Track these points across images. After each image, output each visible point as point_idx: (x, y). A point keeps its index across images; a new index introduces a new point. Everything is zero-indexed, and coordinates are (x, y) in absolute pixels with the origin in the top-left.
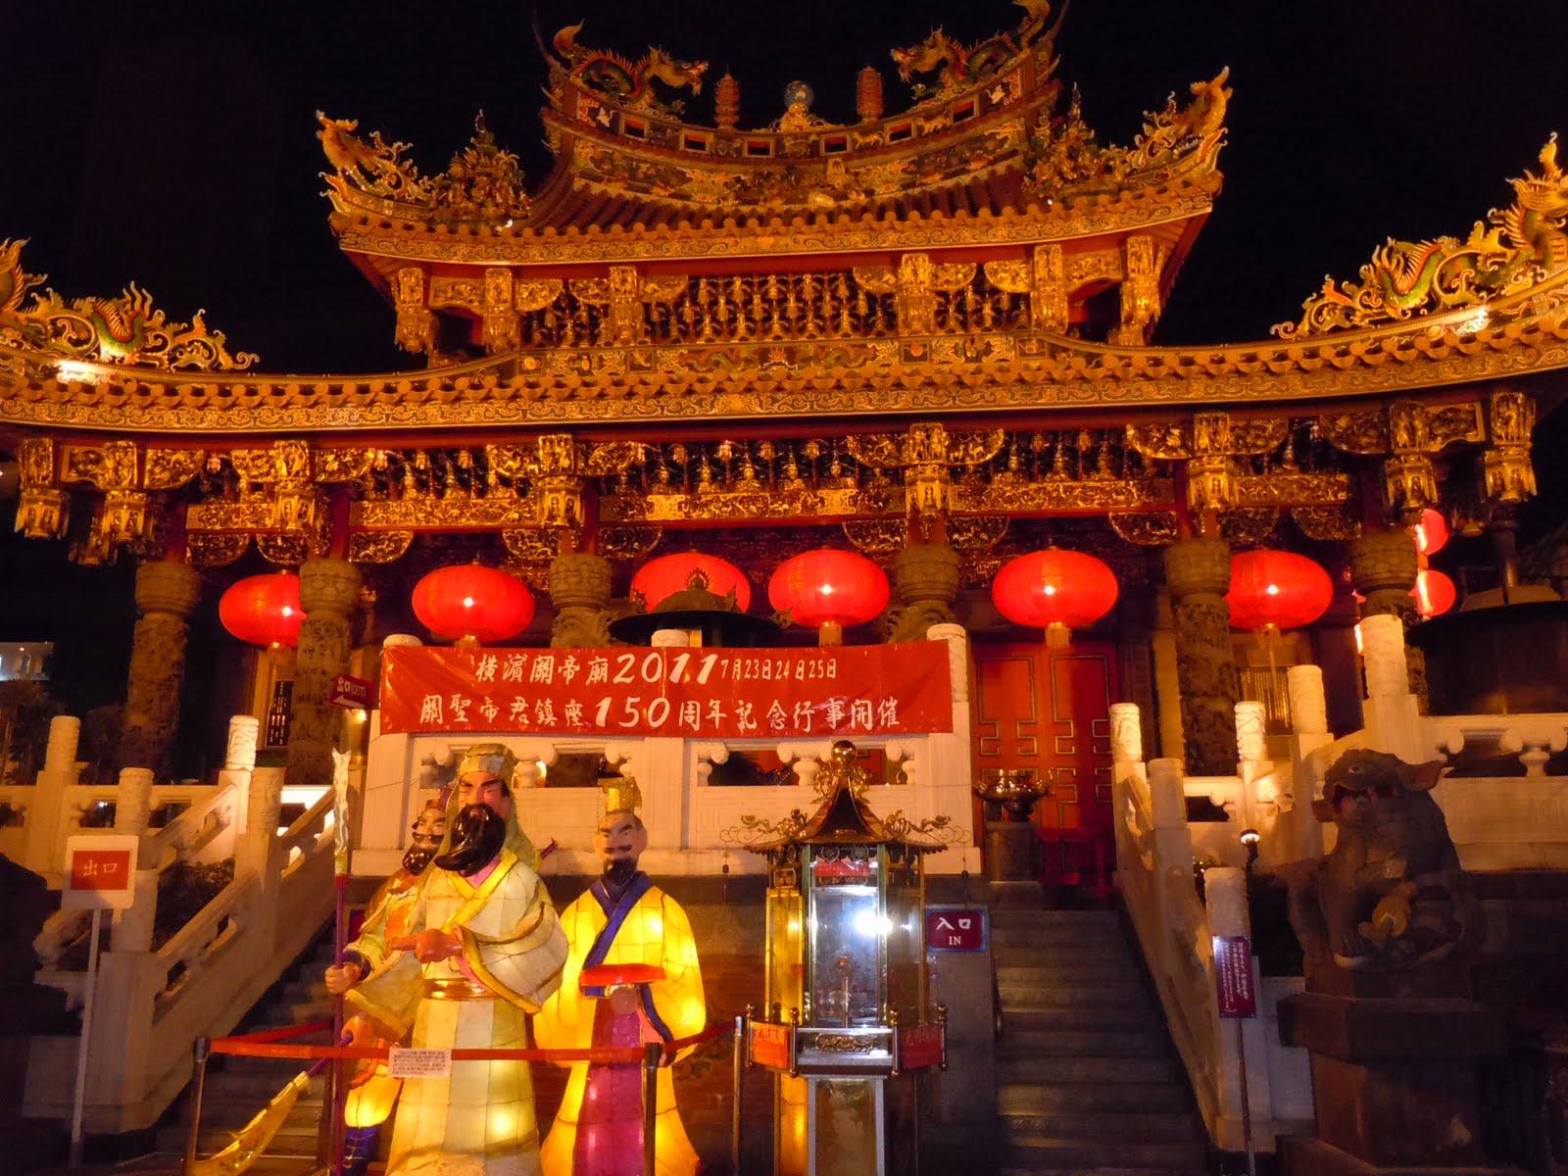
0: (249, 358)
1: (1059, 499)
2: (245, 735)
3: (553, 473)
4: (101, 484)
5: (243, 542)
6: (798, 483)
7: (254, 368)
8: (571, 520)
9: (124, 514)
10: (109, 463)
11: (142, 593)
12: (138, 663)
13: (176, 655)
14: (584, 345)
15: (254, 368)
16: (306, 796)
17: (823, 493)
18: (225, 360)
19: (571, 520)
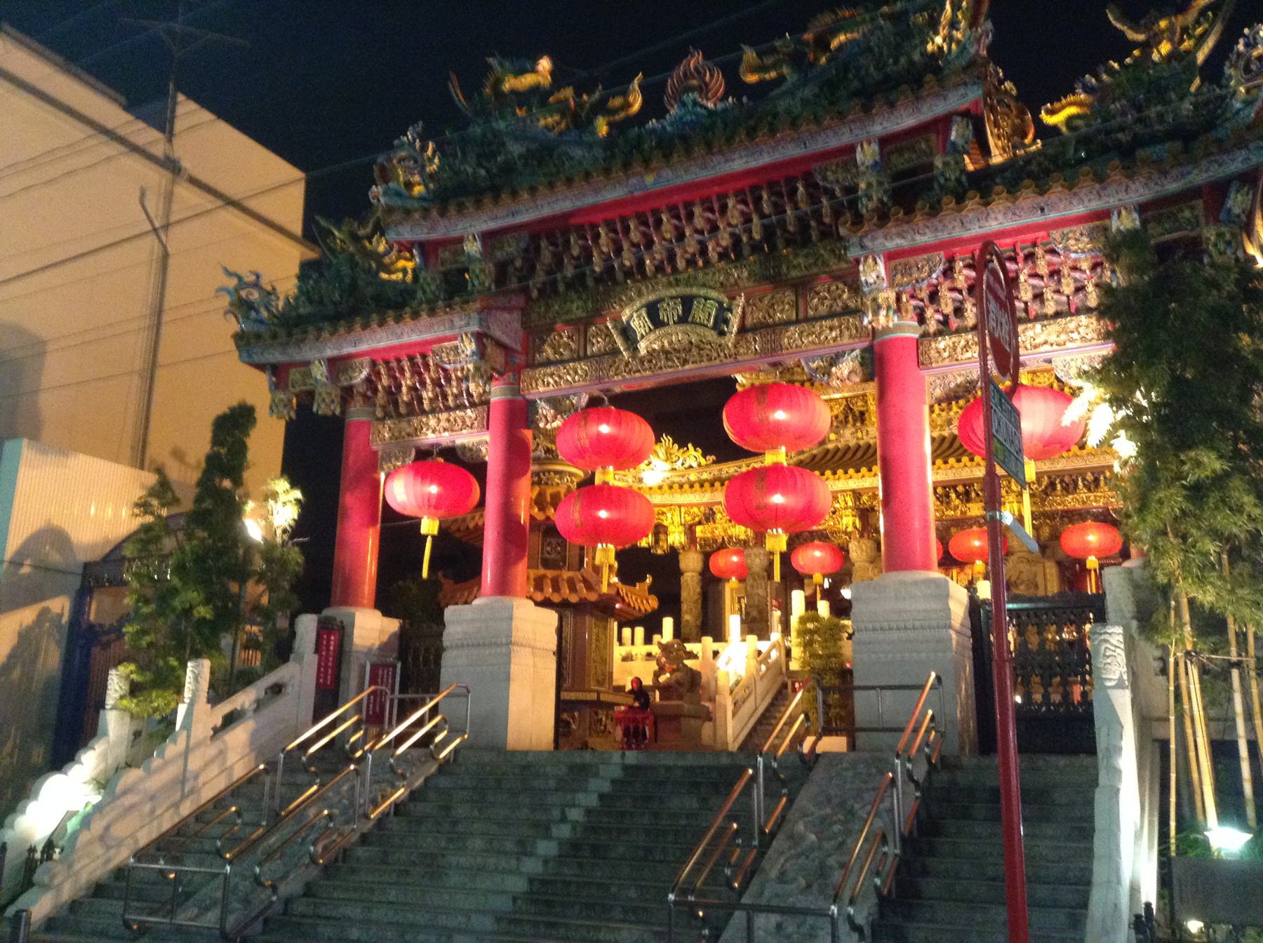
0: (711, 458)
1: (1084, 503)
2: (733, 623)
3: (846, 508)
4: (666, 523)
5: (720, 540)
6: (957, 502)
7: (714, 462)
8: (855, 527)
9: (677, 535)
10: (669, 515)
11: (682, 565)
12: (684, 594)
13: (698, 590)
14: (858, 424)
15: (714, 462)
16: (764, 646)
17: (969, 505)
18: (703, 461)
19: (855, 527)
